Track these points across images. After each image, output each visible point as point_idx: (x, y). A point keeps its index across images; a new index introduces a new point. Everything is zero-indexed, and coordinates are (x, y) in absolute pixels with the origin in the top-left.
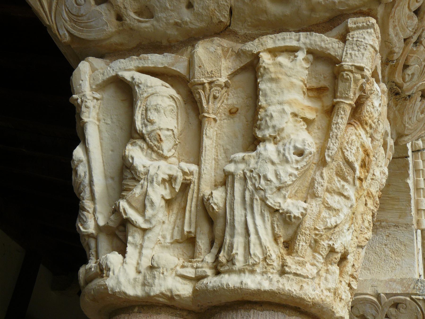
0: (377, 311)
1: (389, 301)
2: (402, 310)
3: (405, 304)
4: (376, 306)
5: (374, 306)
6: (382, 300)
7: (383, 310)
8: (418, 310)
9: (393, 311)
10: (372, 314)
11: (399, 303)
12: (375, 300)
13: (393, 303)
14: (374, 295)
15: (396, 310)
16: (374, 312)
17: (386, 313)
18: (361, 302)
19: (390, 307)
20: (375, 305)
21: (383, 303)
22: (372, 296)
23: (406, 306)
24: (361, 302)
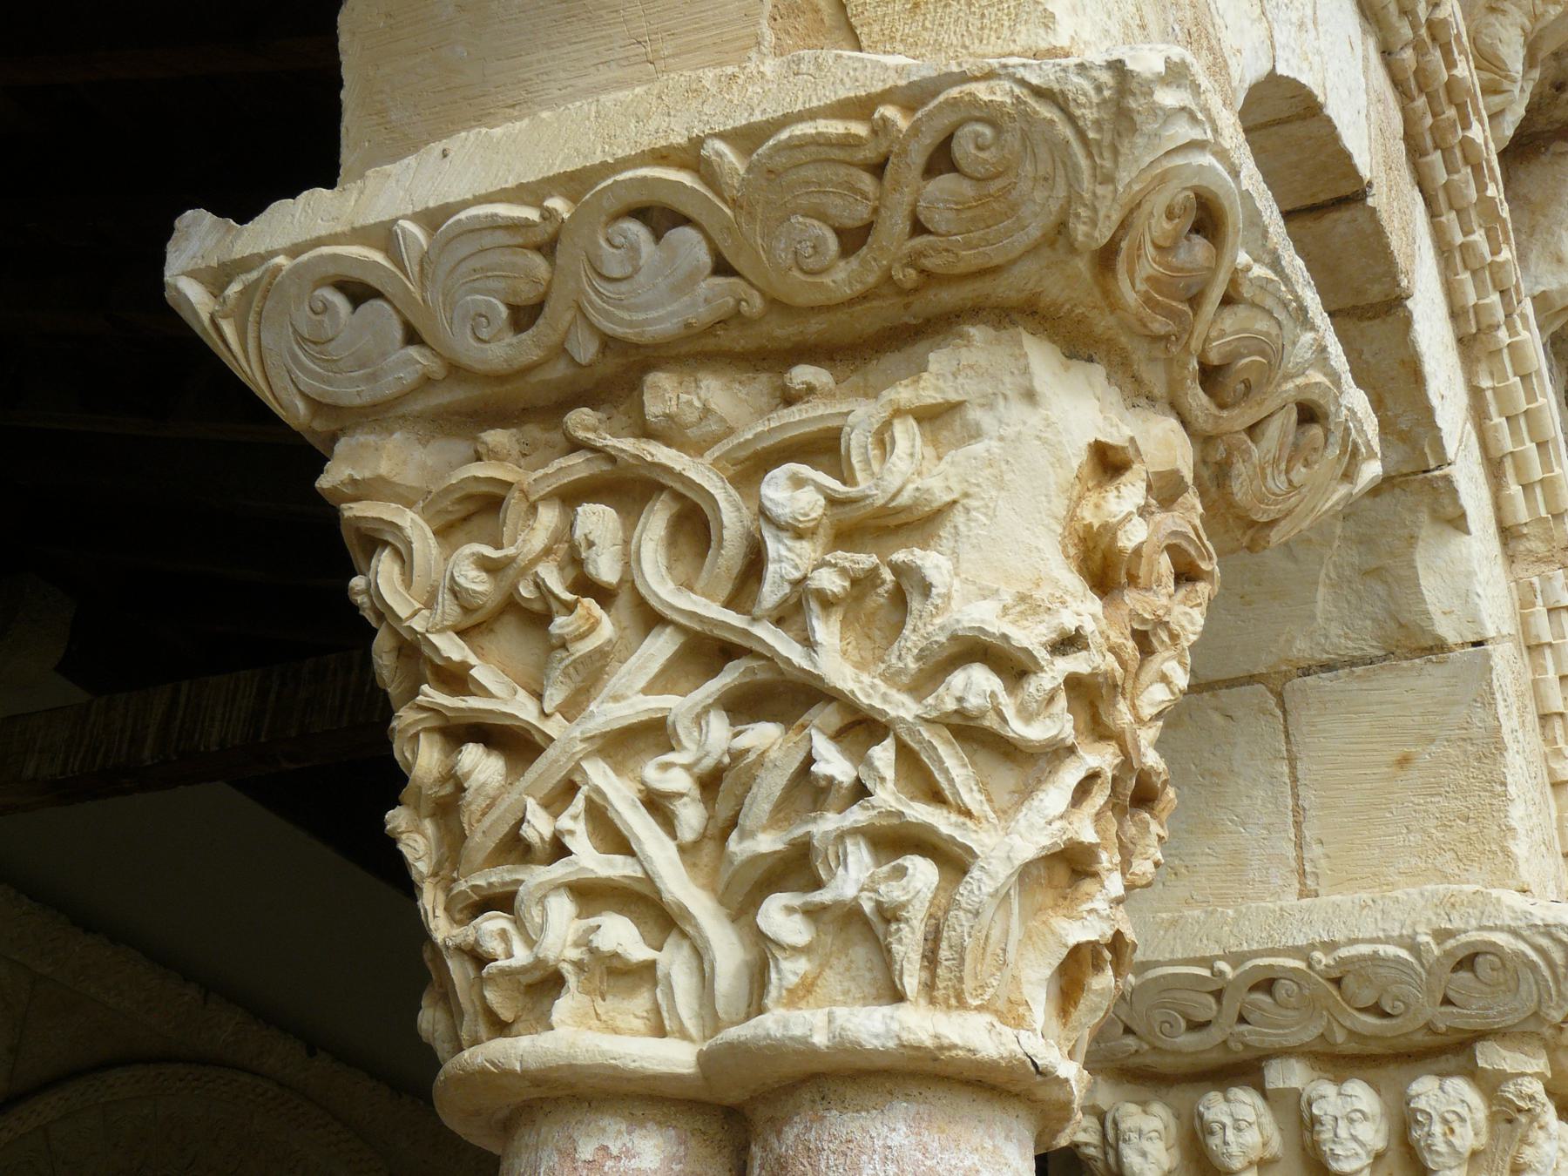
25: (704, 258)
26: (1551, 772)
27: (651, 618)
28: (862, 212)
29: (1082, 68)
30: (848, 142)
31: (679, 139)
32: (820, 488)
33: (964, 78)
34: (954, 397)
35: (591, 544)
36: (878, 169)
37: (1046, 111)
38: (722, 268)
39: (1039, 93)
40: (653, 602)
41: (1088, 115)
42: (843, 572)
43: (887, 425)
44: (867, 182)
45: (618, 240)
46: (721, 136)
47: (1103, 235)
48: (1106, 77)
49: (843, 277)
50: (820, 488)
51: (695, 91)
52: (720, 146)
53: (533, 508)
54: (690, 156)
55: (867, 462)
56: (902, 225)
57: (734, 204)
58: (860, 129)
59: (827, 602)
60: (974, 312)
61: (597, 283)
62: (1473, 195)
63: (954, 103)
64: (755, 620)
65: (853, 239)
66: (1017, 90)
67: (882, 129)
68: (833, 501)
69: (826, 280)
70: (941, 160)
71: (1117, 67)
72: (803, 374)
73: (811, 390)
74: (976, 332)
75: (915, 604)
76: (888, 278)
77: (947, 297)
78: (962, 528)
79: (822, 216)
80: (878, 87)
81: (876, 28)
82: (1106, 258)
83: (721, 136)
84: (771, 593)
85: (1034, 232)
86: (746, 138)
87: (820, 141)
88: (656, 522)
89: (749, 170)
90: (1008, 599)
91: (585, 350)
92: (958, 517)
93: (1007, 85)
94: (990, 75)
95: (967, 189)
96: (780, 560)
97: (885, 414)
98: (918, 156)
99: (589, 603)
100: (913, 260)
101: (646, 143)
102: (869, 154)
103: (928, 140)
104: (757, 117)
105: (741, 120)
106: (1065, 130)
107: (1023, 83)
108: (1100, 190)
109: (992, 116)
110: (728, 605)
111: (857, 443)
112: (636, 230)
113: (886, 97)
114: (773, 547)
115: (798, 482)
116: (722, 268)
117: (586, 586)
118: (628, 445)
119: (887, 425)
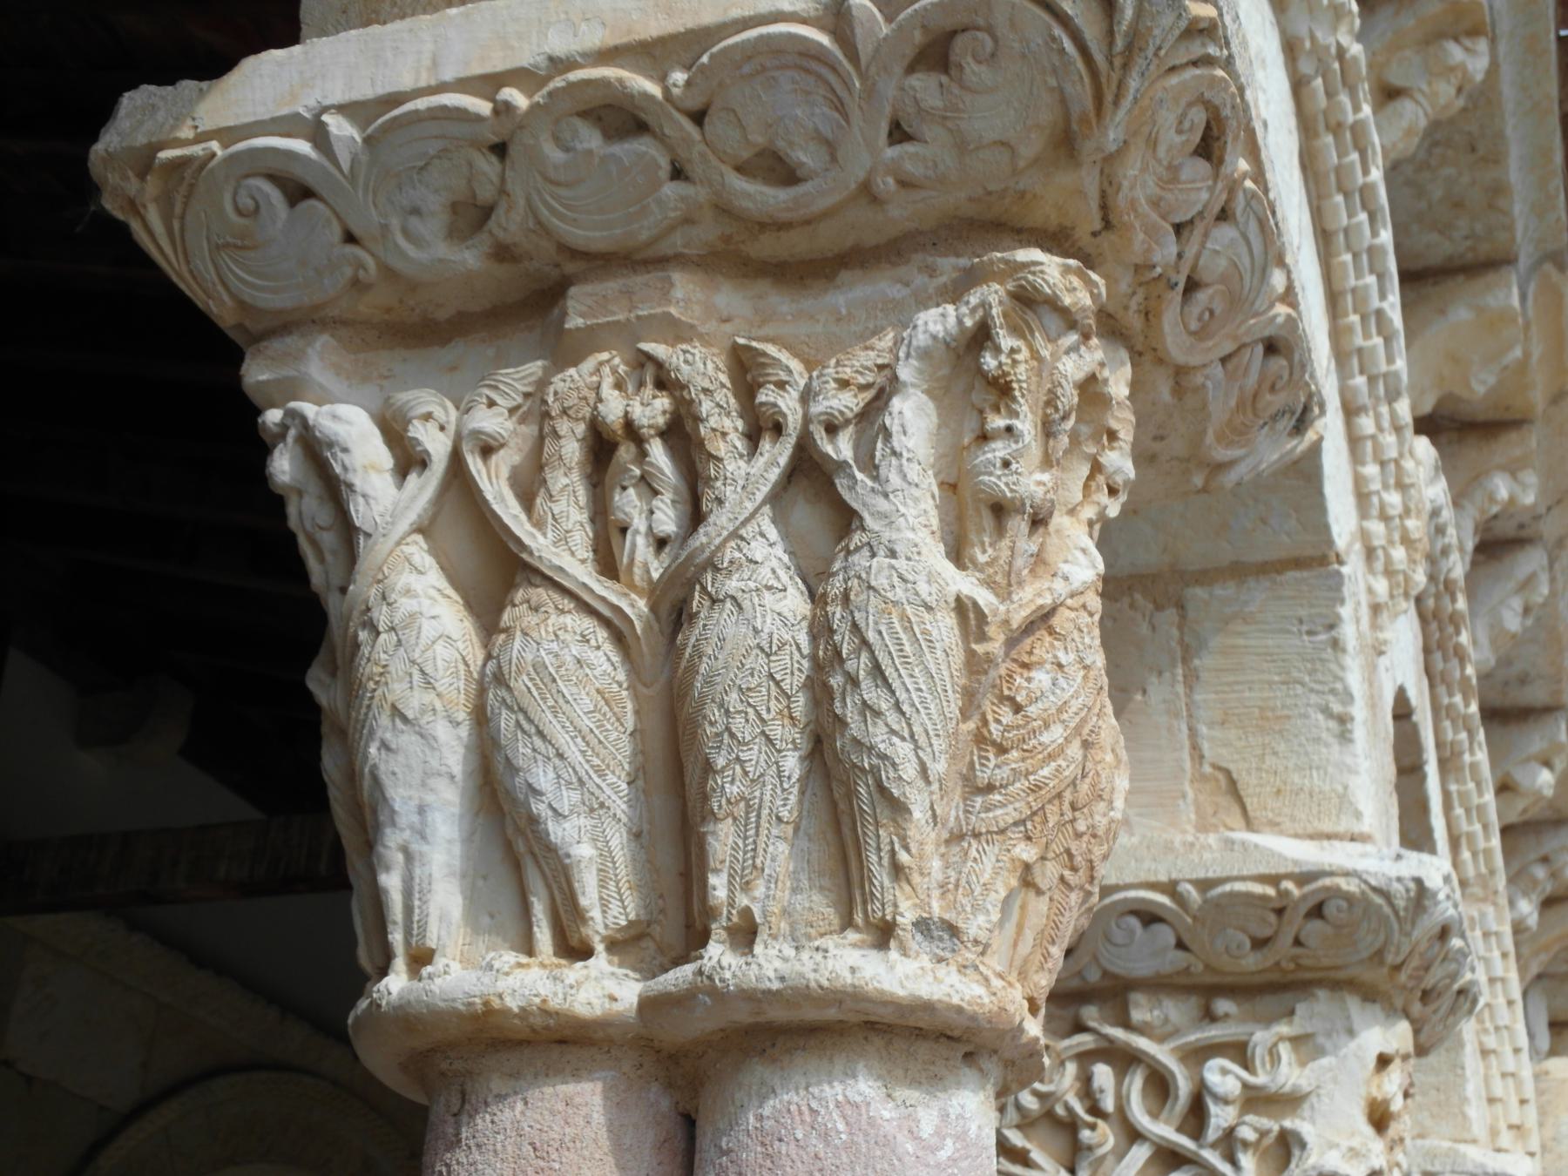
0: (840, 107)
1: (900, 27)
2: (974, 71)
3: (990, 30)
4: (832, 78)
5: (819, 77)
6: (858, 31)
7: (870, 92)
8: (1062, 51)
9: (925, 85)
10: (817, 130)
11: (953, 34)
12: (824, 39)
13: (918, 37)
14: (813, 13)
15: (944, 79)
16: (821, 116)
17: (888, 110)
18: (746, 69)
19: (911, 69)
20: (825, 71)
21: (865, 49)
22: (804, 21)
23: (995, 40)
24: (746, 69)
25: (1172, 941)
26: (1481, 1043)
27: (1134, 1135)
28: (1267, 932)
29: (1399, 879)
30: (1264, 898)
31: (1163, 878)
32: (1238, 1077)
33: (1331, 874)
34: (1309, 1030)
35: (1102, 1091)
36: (1280, 912)
37: (1378, 900)
38: (1180, 945)
39: (1375, 889)
40: (1139, 1127)
41: (1401, 903)
42: (1256, 1129)
43: (1275, 1045)
44: (1272, 918)
45: (1124, 926)
46: (1190, 881)
47: (1399, 960)
48: (1412, 885)
49: (1252, 962)
50: (1238, 1077)
51: (1169, 847)
52: (1189, 887)
53: (1062, 1063)
54: (1170, 888)
55: (1263, 1064)
56: (1290, 940)
57: (1194, 918)
58: (1270, 891)
59: (1246, 1145)
60: (1319, 983)
61: (1109, 947)
62: (1457, 674)
63: (1327, 889)
64: (1201, 1146)
65: (1259, 944)
66: (1363, 886)
67: (1284, 894)
68: (1246, 1086)
69: (1243, 962)
70: (1317, 911)
71: (1419, 882)
72: (1223, 1006)
73: (1227, 1016)
74: (1322, 994)
75: (1296, 1152)
76: (1277, 964)
77: (1308, 975)
78: (1316, 1105)
79: (1244, 931)
80: (1282, 870)
81: (1255, 800)
82: (1397, 968)
83: (1190, 881)
84: (1212, 1134)
85: (1365, 954)
86: (1204, 885)
87: (1249, 896)
88: (1136, 1083)
89: (1205, 901)
90: (1344, 1149)
91: (1094, 976)
92: (1313, 1099)
93: (1357, 881)
94: (1347, 874)
95: (1328, 930)
96: (1217, 1116)
97: (1274, 1039)
98: (1304, 909)
99: (1101, 1123)
100: (1294, 959)
101: (1143, 877)
102: (1277, 905)
103: (1311, 903)
104: (1211, 875)
105: (1201, 874)
106: (1387, 910)
107: (1366, 882)
108: (1403, 939)
109: (1348, 897)
110: (1180, 1130)
111: (1260, 1053)
112: (1134, 922)
113: (1288, 876)
114: (1213, 1108)
115: (1224, 1072)
116: (1180, 945)
117: (1095, 1110)
118: (1118, 1033)
119: (1275, 1045)
